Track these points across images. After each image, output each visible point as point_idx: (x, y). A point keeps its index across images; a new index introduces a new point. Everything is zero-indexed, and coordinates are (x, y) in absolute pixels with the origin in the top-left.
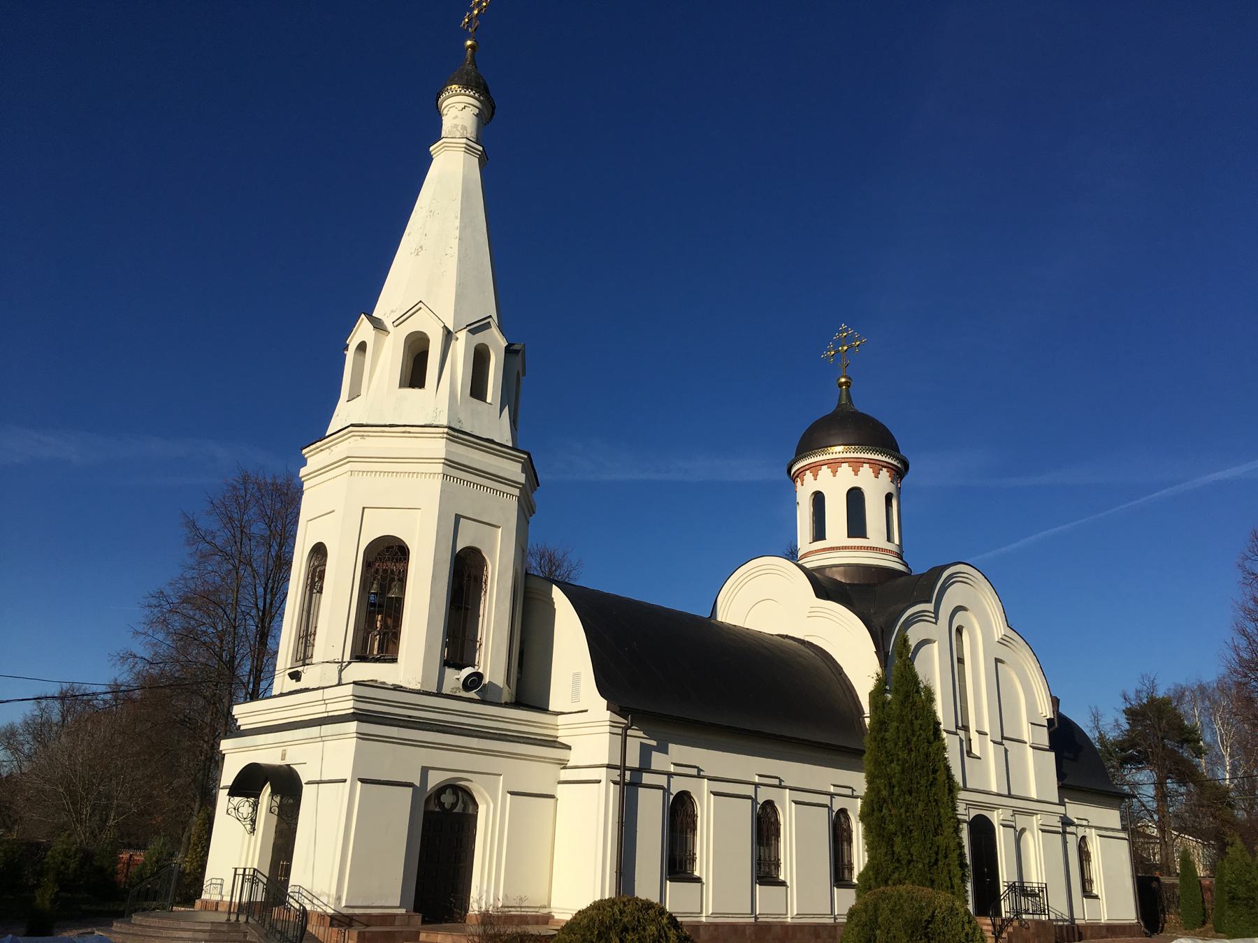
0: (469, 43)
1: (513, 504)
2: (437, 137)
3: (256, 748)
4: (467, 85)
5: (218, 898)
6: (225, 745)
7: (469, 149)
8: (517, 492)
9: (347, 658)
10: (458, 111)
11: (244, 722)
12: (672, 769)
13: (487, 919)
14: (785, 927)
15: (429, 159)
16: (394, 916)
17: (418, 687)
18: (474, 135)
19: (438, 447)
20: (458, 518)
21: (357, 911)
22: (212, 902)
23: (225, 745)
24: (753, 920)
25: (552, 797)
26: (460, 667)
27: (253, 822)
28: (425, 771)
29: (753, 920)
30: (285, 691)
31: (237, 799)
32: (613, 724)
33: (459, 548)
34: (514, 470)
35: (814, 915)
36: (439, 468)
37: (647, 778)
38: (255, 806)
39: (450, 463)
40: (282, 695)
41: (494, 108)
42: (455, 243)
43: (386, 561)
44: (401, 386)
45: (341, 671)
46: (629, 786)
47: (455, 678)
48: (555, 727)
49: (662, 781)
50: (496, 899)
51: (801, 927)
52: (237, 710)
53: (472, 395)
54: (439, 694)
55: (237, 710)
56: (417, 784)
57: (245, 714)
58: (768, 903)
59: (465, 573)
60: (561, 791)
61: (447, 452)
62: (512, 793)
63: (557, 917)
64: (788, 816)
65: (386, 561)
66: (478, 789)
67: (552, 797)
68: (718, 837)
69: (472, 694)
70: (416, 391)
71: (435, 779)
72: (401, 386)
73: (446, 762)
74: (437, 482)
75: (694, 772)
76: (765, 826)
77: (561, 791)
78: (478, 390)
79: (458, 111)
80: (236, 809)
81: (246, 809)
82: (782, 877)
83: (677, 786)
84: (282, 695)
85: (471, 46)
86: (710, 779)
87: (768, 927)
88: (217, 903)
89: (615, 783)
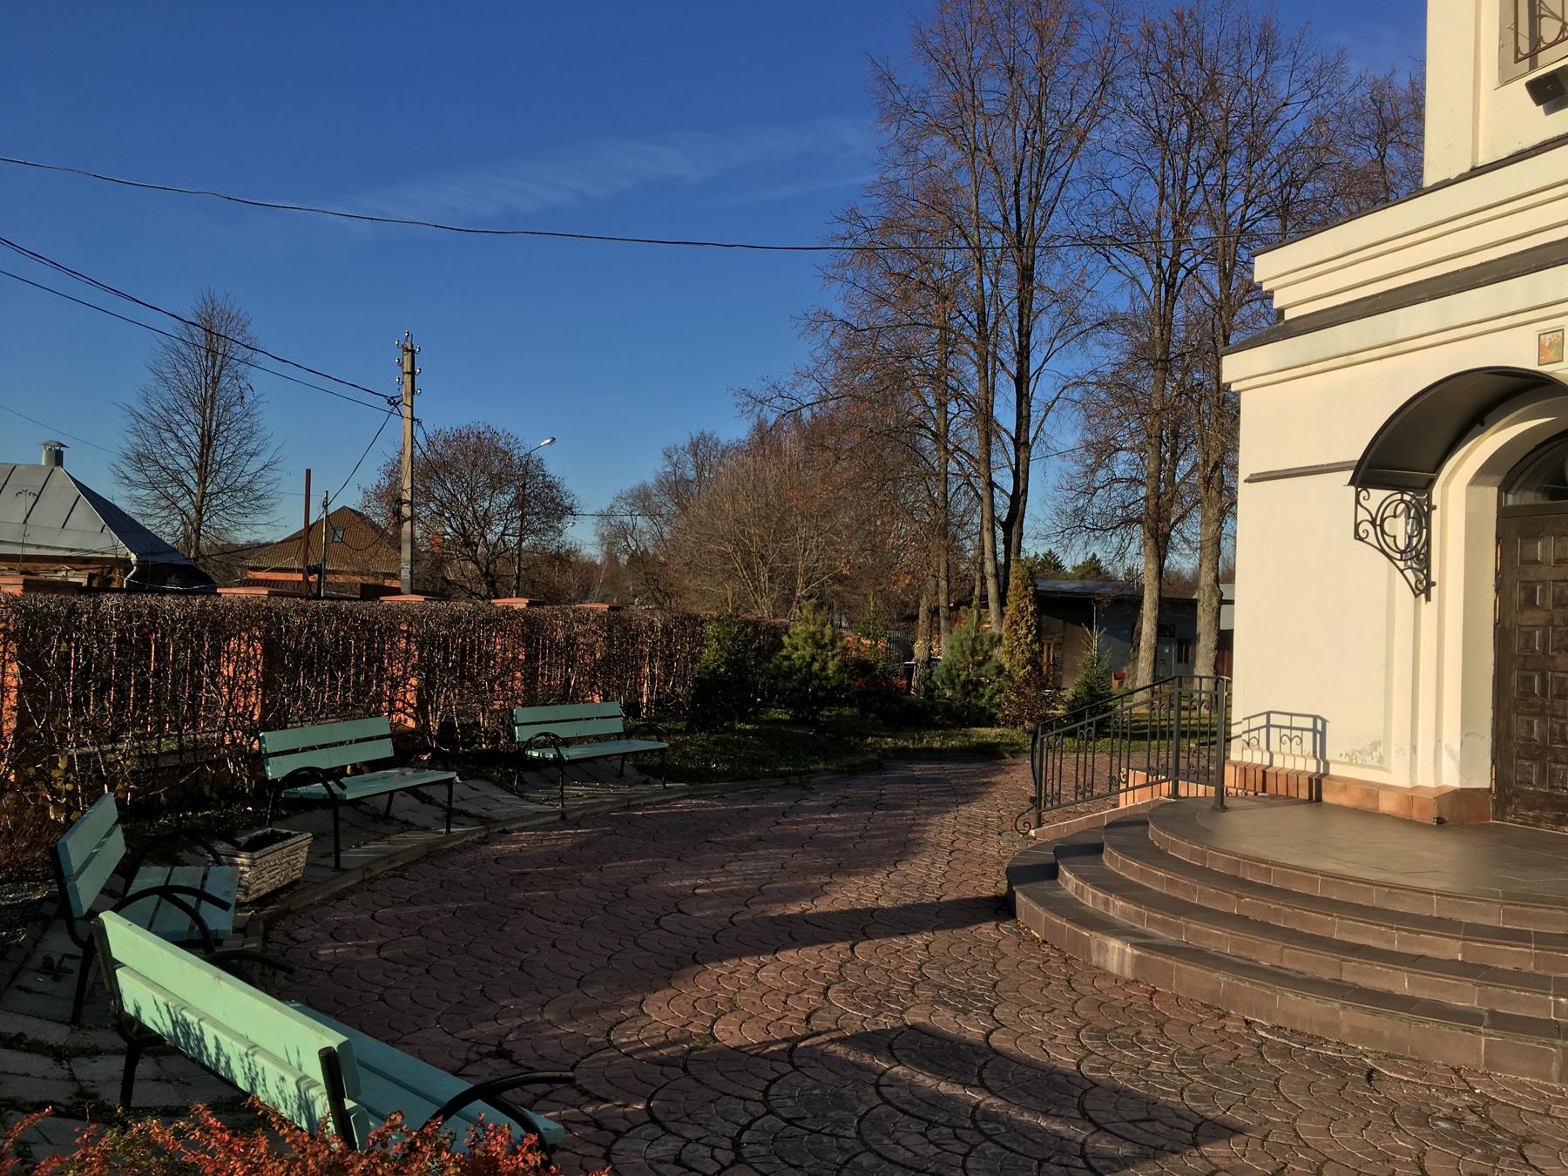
3: (1394, 348)
5: (1312, 767)
6: (1234, 368)
11: (1292, 299)
22: (1291, 777)
23: (1234, 368)
27: (1418, 557)
30: (1483, 160)
31: (1377, 496)
38: (1421, 517)
40: (1476, 172)
52: (1267, 267)
55: (1267, 267)
57: (1290, 272)
80: (1377, 522)
81: (1399, 528)
84: (1476, 172)
88: (1317, 783)
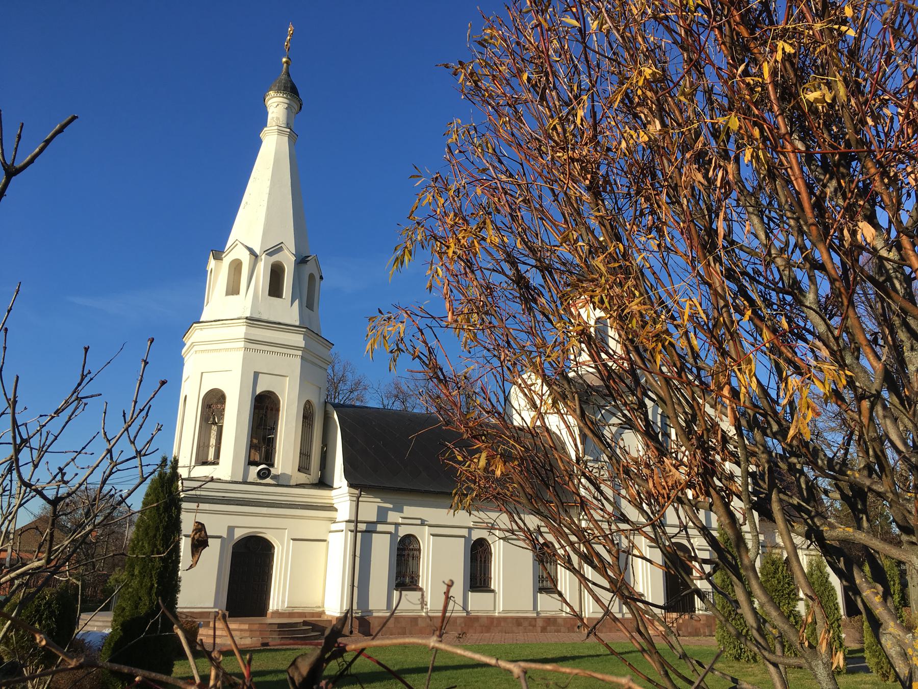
0: (284, 60)
1: (299, 360)
2: (266, 126)
4: (278, 90)
7: (280, 132)
8: (300, 353)
9: (193, 464)
10: (276, 106)
12: (400, 521)
13: (272, 613)
14: (491, 619)
15: (259, 142)
16: (210, 613)
17: (229, 479)
18: (285, 122)
19: (241, 331)
20: (256, 375)
21: (185, 610)
24: (465, 614)
25: (325, 541)
26: (257, 464)
28: (231, 529)
29: (465, 614)
32: (351, 495)
33: (258, 392)
34: (298, 340)
35: (518, 611)
36: (242, 344)
37: (380, 527)
39: (249, 340)
41: (300, 100)
42: (265, 197)
43: (213, 404)
44: (227, 294)
45: (190, 472)
46: (363, 533)
47: (254, 470)
48: (331, 498)
49: (391, 528)
50: (283, 602)
51: (505, 619)
53: (270, 295)
54: (245, 482)
56: (225, 536)
58: (478, 603)
59: (264, 408)
60: (331, 537)
61: (246, 334)
62: (294, 540)
63: (327, 613)
64: (498, 549)
65: (213, 404)
66: (270, 536)
67: (325, 541)
68: (440, 563)
69: (268, 480)
70: (235, 296)
71: (239, 534)
72: (228, 293)
73: (246, 523)
74: (241, 353)
75: (419, 522)
76: (478, 556)
77: (331, 537)
78: (275, 289)
79: (276, 106)
82: (492, 587)
83: (403, 531)
85: (287, 62)
86: (430, 526)
87: (477, 619)
89: (351, 531)
